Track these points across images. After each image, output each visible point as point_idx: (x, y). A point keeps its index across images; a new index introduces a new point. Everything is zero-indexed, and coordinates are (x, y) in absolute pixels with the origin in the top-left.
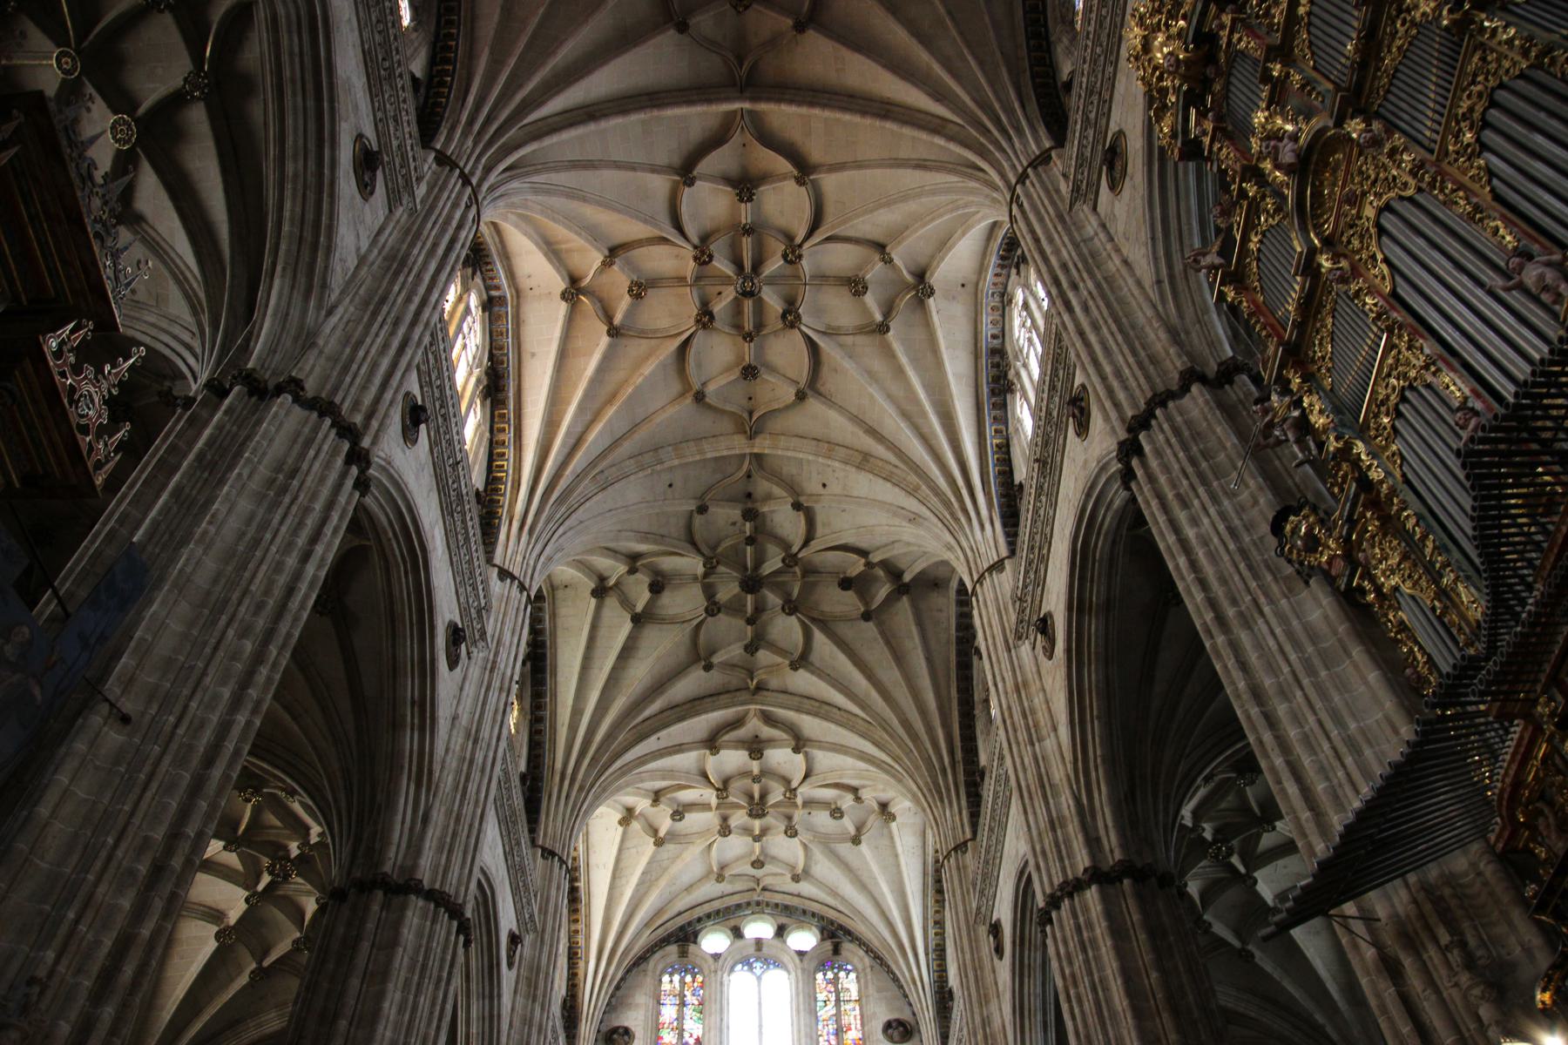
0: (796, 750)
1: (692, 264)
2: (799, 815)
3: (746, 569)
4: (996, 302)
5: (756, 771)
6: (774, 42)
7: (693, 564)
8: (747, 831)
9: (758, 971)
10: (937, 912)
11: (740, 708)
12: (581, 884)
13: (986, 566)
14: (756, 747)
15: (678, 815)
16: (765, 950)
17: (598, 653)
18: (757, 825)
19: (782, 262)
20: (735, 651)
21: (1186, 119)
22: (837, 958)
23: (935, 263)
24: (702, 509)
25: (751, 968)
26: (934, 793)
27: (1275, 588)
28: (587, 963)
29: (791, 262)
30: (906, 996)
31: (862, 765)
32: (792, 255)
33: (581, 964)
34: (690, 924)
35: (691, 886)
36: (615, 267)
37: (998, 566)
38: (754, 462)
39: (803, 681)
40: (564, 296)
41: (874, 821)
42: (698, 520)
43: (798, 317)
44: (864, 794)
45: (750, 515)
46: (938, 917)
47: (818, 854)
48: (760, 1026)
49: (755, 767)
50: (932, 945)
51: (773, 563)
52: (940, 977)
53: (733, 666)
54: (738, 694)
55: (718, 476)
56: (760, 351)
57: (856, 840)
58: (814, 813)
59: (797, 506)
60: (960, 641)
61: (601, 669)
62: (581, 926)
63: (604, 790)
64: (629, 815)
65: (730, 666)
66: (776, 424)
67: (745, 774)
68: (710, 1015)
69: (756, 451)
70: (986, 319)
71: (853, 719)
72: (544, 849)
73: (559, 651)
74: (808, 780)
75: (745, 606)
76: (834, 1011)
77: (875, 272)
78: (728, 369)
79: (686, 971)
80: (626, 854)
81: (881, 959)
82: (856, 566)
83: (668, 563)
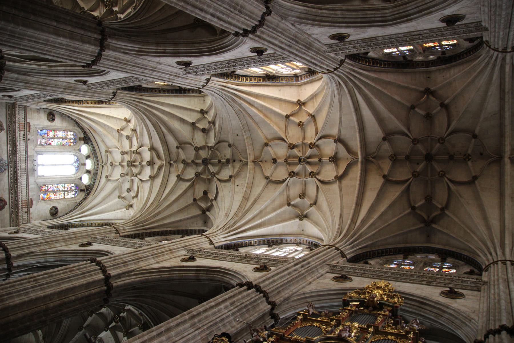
0: (150, 177)
1: (309, 142)
2: (128, 178)
3: (210, 160)
5: (143, 163)
6: (380, 168)
7: (212, 142)
8: (123, 161)
9: (75, 164)
10: (95, 224)
12: (104, 105)
13: (212, 239)
14: (151, 163)
15: (128, 137)
16: (82, 167)
17: (182, 111)
18: (125, 164)
19: (310, 171)
20: (183, 156)
21: (356, 301)
22: (79, 190)
23: (310, 221)
24: (230, 146)
25: (76, 162)
26: (136, 223)
27: (204, 335)
28: (77, 107)
29: (310, 174)
30: (66, 214)
31: (145, 199)
32: (312, 175)
33: (77, 105)
34: (91, 141)
35: (104, 142)
36: (308, 117)
37: (211, 243)
39: (173, 179)
40: (299, 101)
41: (126, 203)
42: (226, 144)
43: (292, 177)
44: (135, 199)
45: (228, 161)
46: (94, 225)
47: (115, 184)
48: (55, 165)
49: (144, 163)
50: (84, 223)
51: (212, 169)
52: (73, 226)
53: (178, 156)
54: (169, 157)
55: (240, 151)
56: (281, 164)
57: (120, 197)
58: (129, 183)
59: (231, 177)
60: (187, 231)
62: (90, 105)
63: (136, 113)
64: (128, 121)
65: (178, 155)
66: (257, 170)
67: (142, 160)
68: (59, 148)
69: (249, 163)
70: (292, 238)
71: (161, 196)
72: (116, 92)
75: (198, 160)
76: (61, 190)
78: (275, 154)
79: (74, 140)
80: (115, 120)
81: (79, 206)
82: (211, 196)
83: (212, 134)
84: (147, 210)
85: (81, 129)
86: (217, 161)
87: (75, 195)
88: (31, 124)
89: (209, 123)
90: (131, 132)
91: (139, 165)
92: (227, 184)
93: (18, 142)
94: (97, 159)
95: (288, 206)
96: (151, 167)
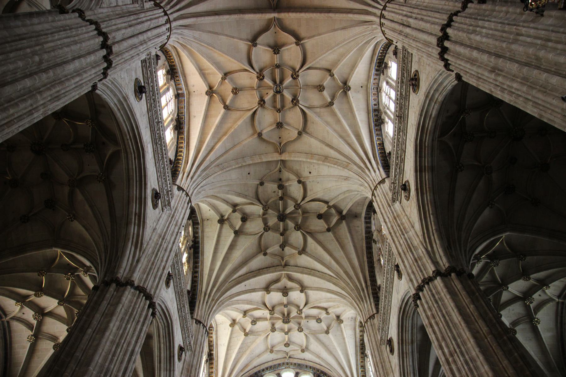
0: (302, 291)
2: (303, 322)
3: (280, 211)
4: (375, 91)
7: (257, 209)
8: (282, 330)
10: (362, 362)
11: (278, 273)
12: (214, 352)
14: (285, 291)
15: (254, 322)
17: (221, 247)
18: (286, 326)
19: (291, 79)
20: (275, 248)
24: (262, 184)
31: (329, 295)
32: (295, 76)
34: (259, 371)
35: (260, 355)
36: (226, 81)
38: (282, 164)
39: (304, 260)
41: (334, 324)
42: (261, 189)
44: (330, 311)
45: (281, 187)
46: (362, 364)
47: (312, 339)
49: (285, 300)
51: (290, 209)
53: (276, 255)
54: (278, 267)
55: (268, 171)
57: (327, 332)
59: (299, 182)
60: (367, 238)
61: (222, 253)
62: (214, 370)
64: (234, 322)
66: (291, 148)
67: (281, 304)
69: (283, 158)
70: (372, 98)
71: (325, 275)
73: (205, 246)
74: (307, 305)
75: (279, 228)
77: (327, 82)
80: (232, 340)
82: (323, 208)
84: (343, 289)
86: (280, 202)
89: (234, 211)
90: (247, 318)
91: (287, 307)
92: (309, 187)
94: (282, 364)
95: (333, 105)
96: (290, 291)
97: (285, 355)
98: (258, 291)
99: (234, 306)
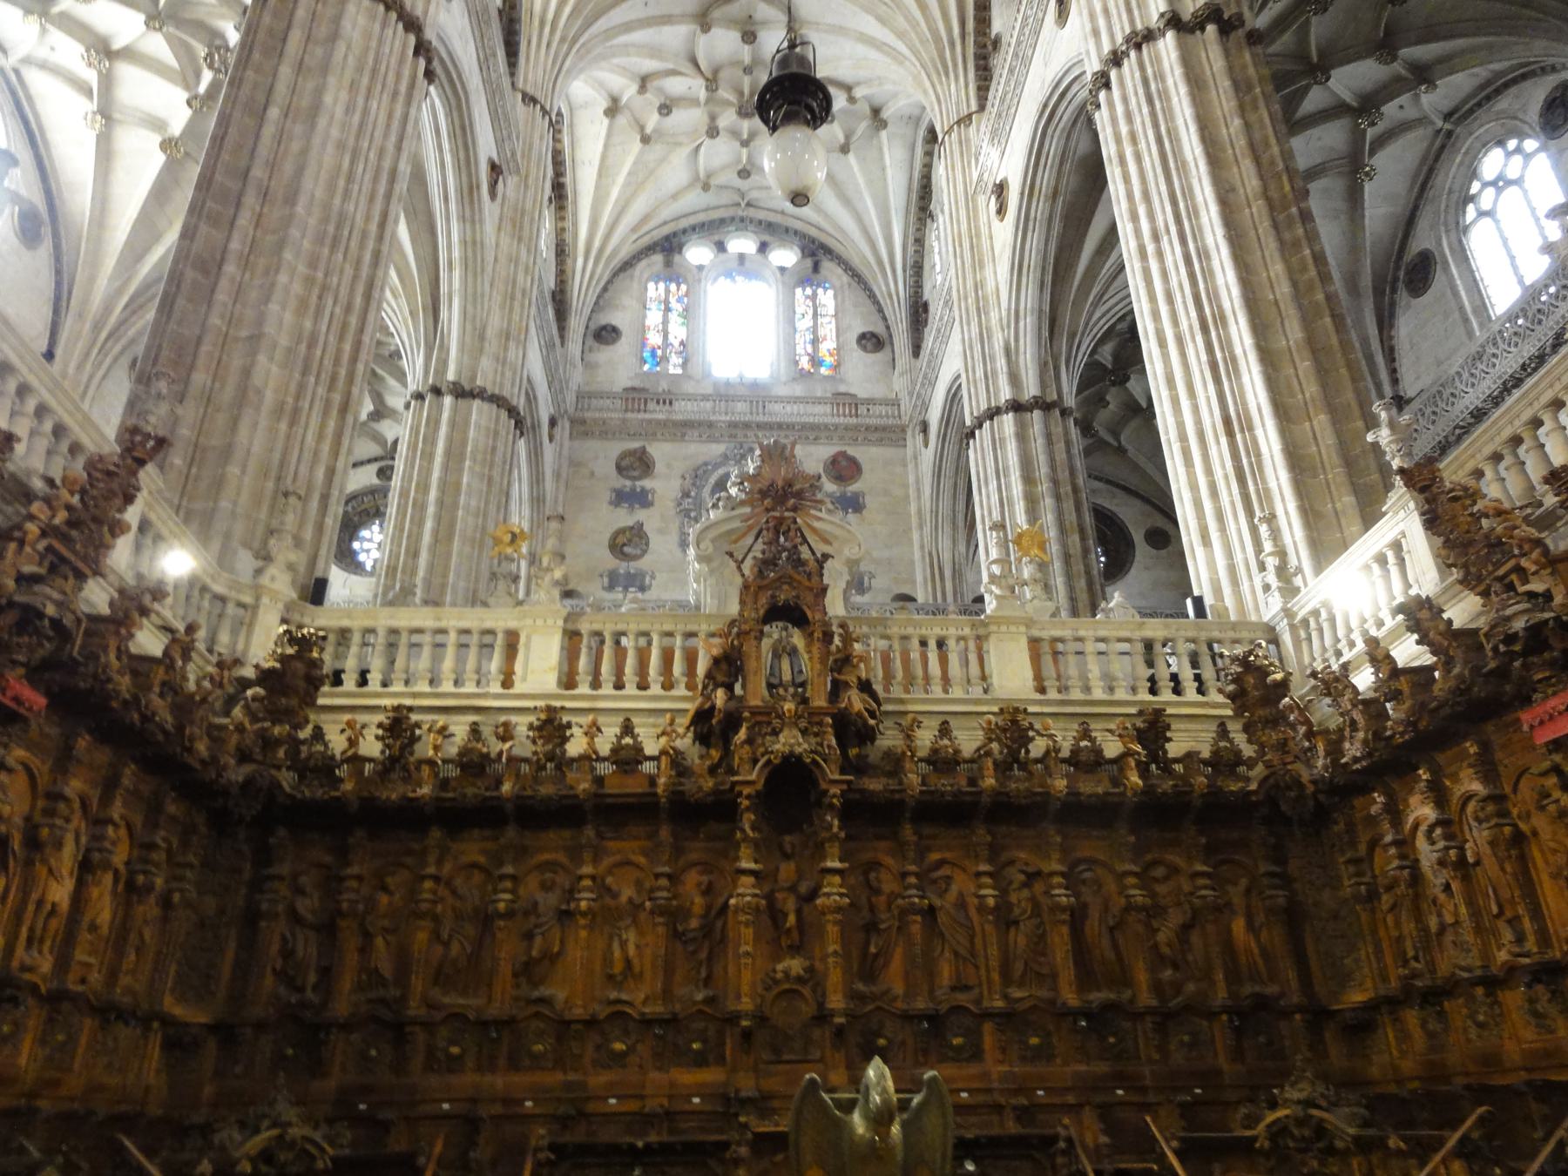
8: (734, 133)
12: (568, 180)
16: (747, 264)
25: (733, 279)
28: (575, 261)
30: (881, 310)
33: (569, 261)
34: (675, 234)
44: (858, 93)
46: (918, 235)
50: (910, 262)
67: (735, 63)
79: (671, 280)
84: (901, 35)
85: (639, 260)
87: (826, 289)
88: (629, 384)
90: (648, 95)
93: (680, 417)
97: (737, 198)
98: (679, 23)
99: (616, 61)
